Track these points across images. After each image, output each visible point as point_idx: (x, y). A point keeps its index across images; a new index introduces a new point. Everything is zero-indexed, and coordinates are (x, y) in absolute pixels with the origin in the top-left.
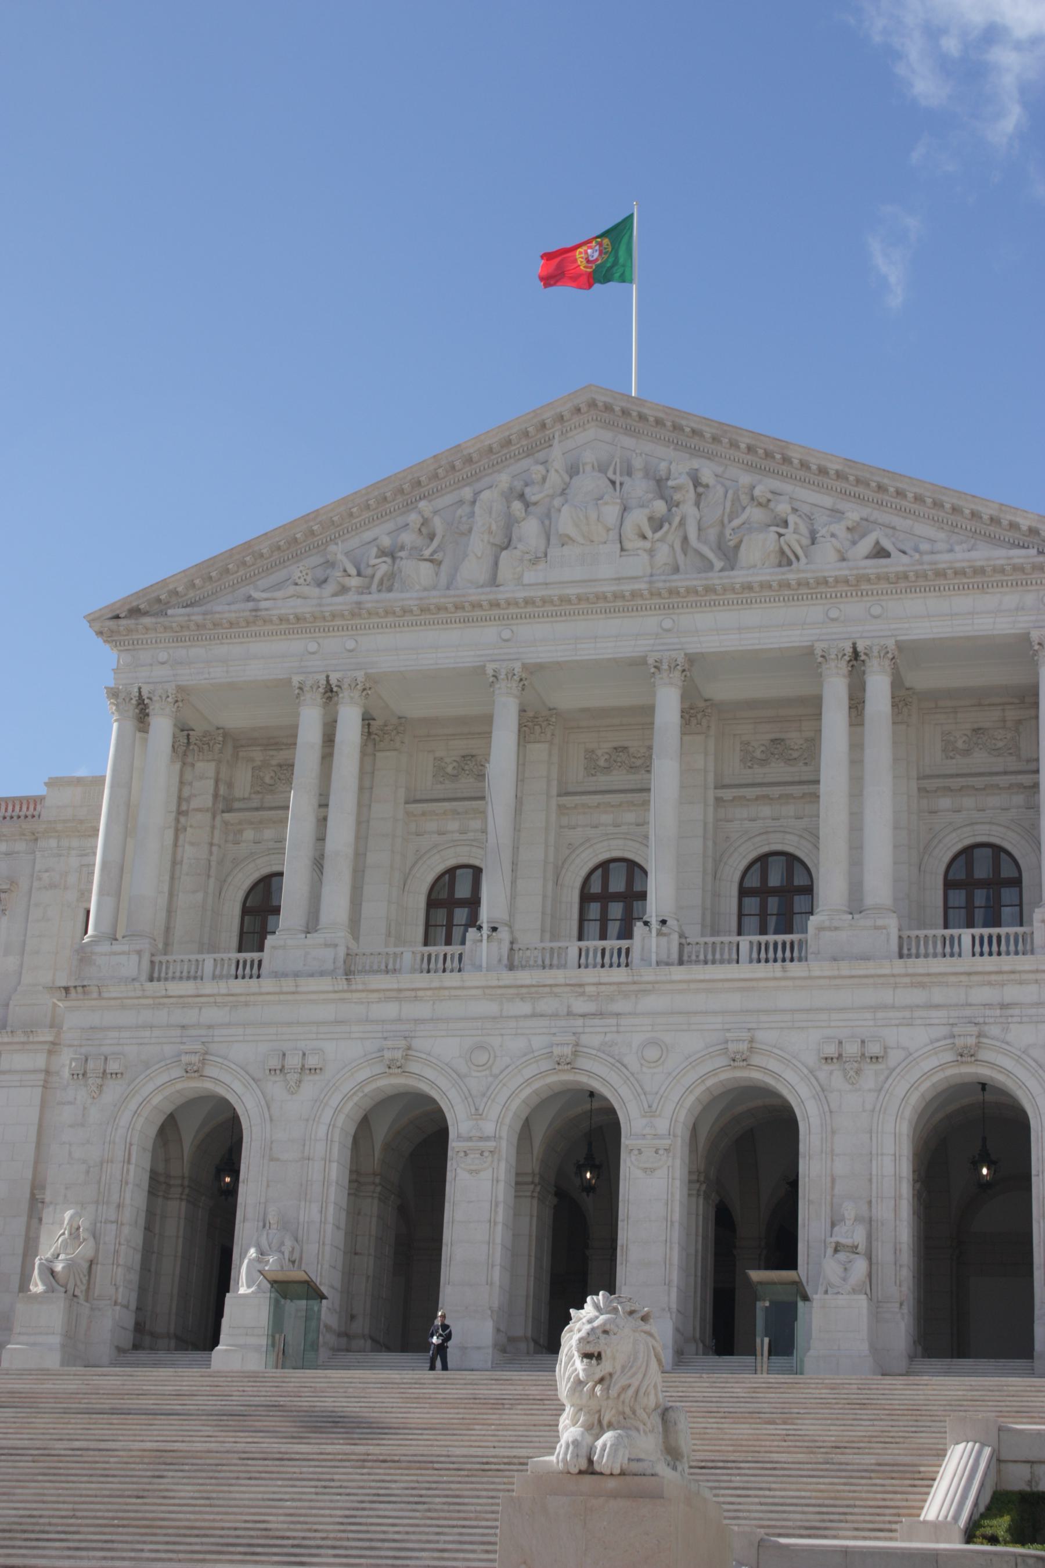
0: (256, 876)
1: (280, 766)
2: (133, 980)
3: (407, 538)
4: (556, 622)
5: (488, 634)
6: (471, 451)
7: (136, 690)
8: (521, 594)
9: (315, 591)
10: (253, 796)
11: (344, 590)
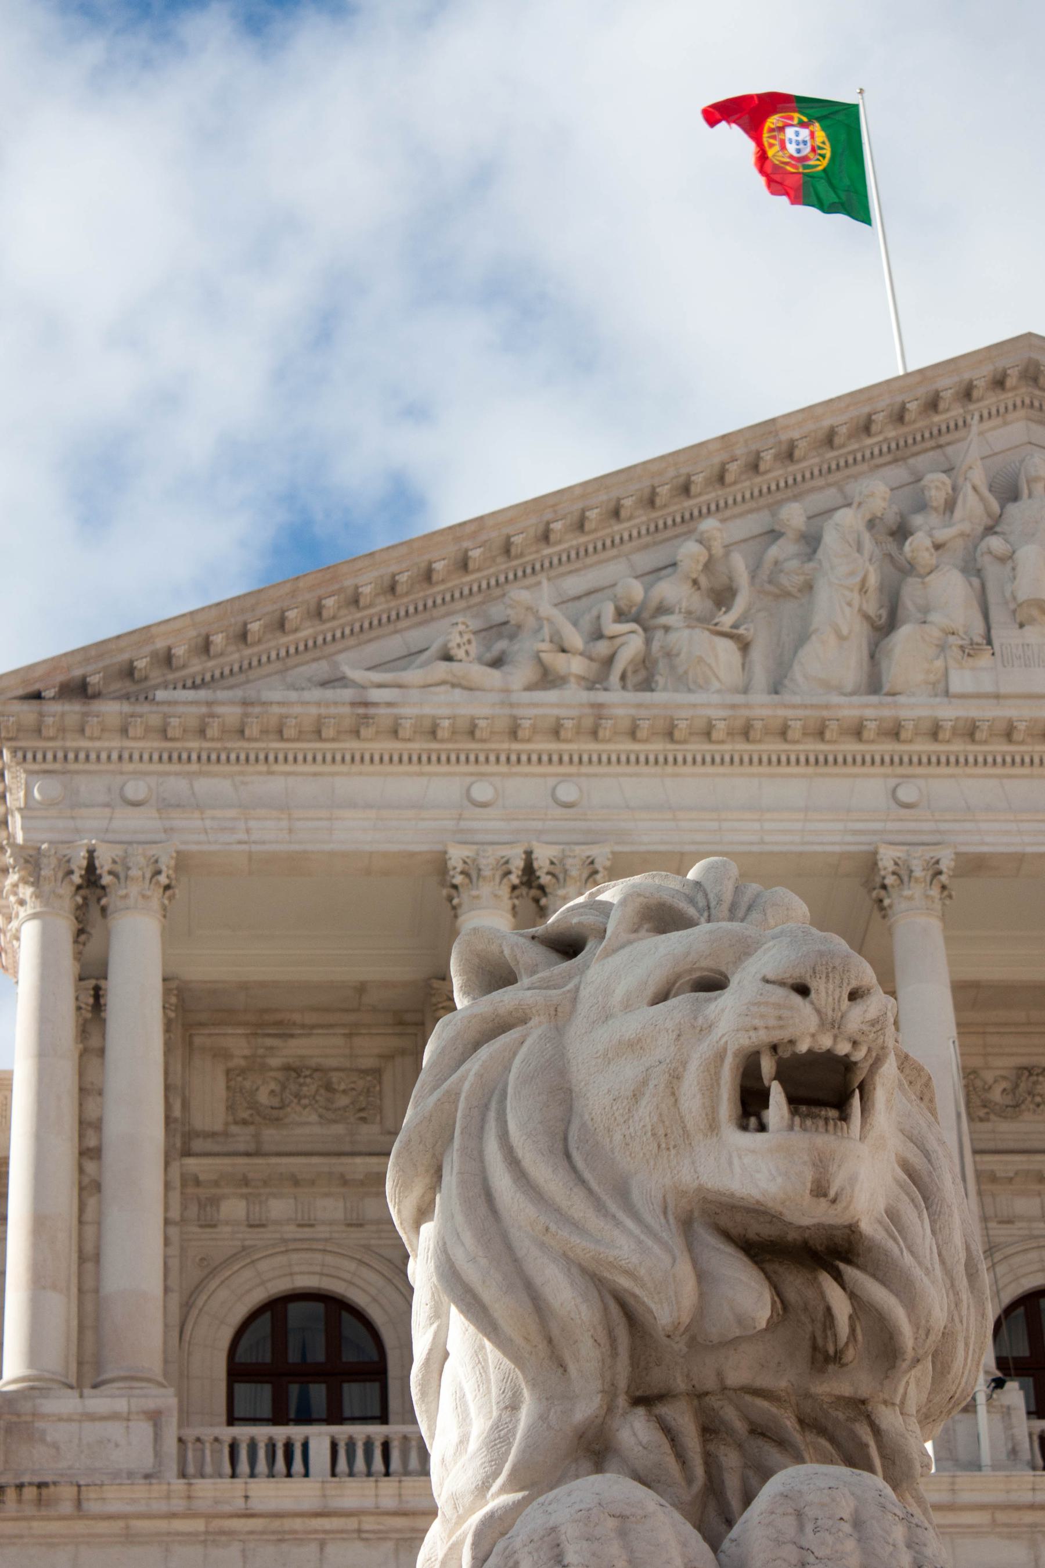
0: (258, 1296)
1: (293, 1070)
2: (147, 1476)
3: (672, 590)
4: (1010, 776)
5: (869, 789)
6: (796, 435)
7: (83, 853)
8: (949, 712)
9: (495, 674)
10: (234, 1129)
11: (547, 679)
